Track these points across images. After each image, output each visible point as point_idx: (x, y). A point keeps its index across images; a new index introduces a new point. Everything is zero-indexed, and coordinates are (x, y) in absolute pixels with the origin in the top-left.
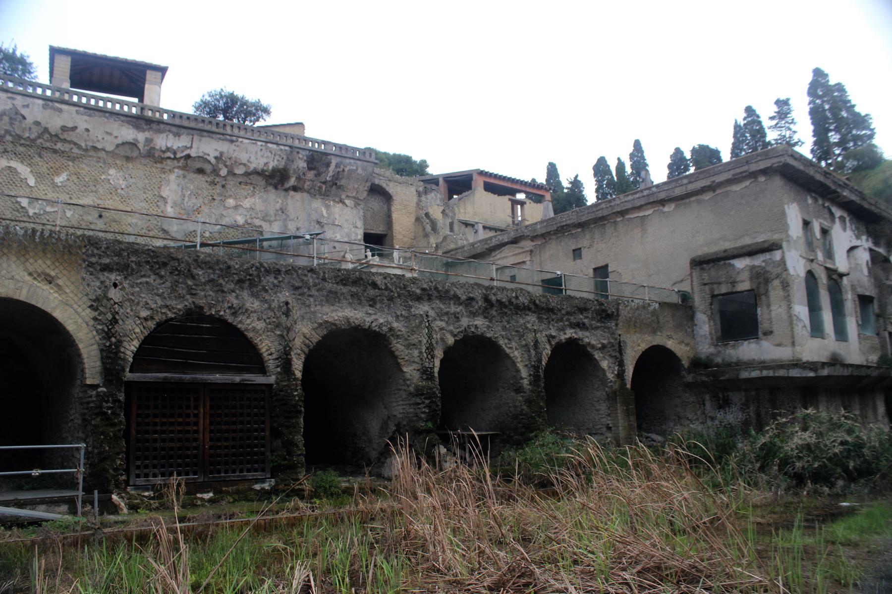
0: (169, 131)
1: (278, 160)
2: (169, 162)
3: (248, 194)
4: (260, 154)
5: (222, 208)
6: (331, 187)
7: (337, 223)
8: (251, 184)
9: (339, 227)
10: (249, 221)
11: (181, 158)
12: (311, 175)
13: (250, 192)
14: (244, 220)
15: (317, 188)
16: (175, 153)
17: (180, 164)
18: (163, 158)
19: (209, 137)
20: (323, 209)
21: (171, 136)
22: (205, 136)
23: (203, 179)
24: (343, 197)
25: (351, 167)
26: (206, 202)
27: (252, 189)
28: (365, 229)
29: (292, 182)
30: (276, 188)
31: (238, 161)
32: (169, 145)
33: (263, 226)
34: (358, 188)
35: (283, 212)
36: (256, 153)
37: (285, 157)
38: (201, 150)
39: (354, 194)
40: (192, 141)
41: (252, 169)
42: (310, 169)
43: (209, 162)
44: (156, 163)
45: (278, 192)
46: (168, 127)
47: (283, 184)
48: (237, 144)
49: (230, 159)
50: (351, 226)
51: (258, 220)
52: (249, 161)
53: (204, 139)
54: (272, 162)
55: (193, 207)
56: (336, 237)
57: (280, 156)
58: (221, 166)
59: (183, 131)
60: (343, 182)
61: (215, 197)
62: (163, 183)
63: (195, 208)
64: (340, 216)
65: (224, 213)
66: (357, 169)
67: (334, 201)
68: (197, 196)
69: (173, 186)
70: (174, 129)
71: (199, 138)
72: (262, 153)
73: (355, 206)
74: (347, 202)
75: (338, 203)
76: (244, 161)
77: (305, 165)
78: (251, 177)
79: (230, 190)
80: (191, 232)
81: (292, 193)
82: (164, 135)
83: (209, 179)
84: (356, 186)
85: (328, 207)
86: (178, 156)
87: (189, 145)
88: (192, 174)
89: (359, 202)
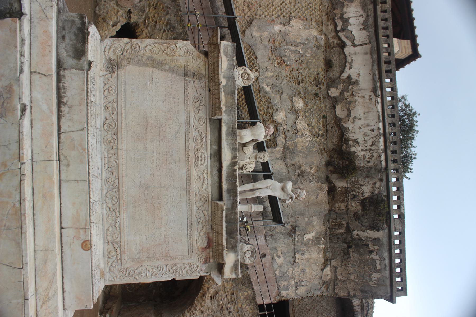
0: (368, 16)
1: (364, 157)
2: (331, 27)
3: (313, 128)
4: (367, 130)
5: (291, 93)
6: (345, 241)
7: (297, 256)
8: (327, 132)
9: (292, 260)
10: (280, 129)
11: (340, 39)
12: (355, 206)
13: (317, 130)
14: (280, 121)
15: (338, 221)
16: (343, 30)
17: (331, 40)
18: (334, 20)
19: (373, 62)
20: (313, 234)
21: (362, 20)
22: (372, 58)
23: (320, 70)
24: (334, 263)
25: (378, 262)
26: (294, 73)
27: (320, 132)
28: (293, 300)
29: (341, 184)
30: (328, 164)
31: (352, 105)
32: (351, 21)
33: (278, 149)
34: (351, 281)
35: (299, 175)
36: (368, 125)
37: (371, 164)
38: (354, 57)
39: (340, 278)
40: (362, 45)
41: (345, 125)
42: (363, 203)
43: (342, 71)
44: (327, 14)
45: (323, 168)
46: (371, 13)
47: (333, 172)
48: (373, 97)
49: (352, 94)
50: (296, 279)
51: (283, 140)
52: (355, 118)
53: (368, 56)
54: (360, 149)
55: (285, 56)
56: (279, 257)
57: (371, 157)
58: (341, 86)
59: (372, 30)
60: (354, 255)
61: (301, 84)
62: (306, 22)
63: (284, 58)
64: (308, 260)
65: (285, 95)
66: (377, 271)
67: (326, 250)
68: (299, 61)
69: (305, 34)
70: (371, 20)
71: (369, 51)
72: (369, 133)
73: (324, 282)
74: (328, 270)
75: (324, 256)
76: (353, 114)
77: (366, 195)
78: (335, 129)
79: (314, 104)
80: (254, 54)
81: (325, 187)
82: (361, 12)
83: (321, 76)
84: (352, 277)
85: (316, 241)
86: (341, 34)
87: (356, 43)
88: (323, 56)
89: (330, 288)
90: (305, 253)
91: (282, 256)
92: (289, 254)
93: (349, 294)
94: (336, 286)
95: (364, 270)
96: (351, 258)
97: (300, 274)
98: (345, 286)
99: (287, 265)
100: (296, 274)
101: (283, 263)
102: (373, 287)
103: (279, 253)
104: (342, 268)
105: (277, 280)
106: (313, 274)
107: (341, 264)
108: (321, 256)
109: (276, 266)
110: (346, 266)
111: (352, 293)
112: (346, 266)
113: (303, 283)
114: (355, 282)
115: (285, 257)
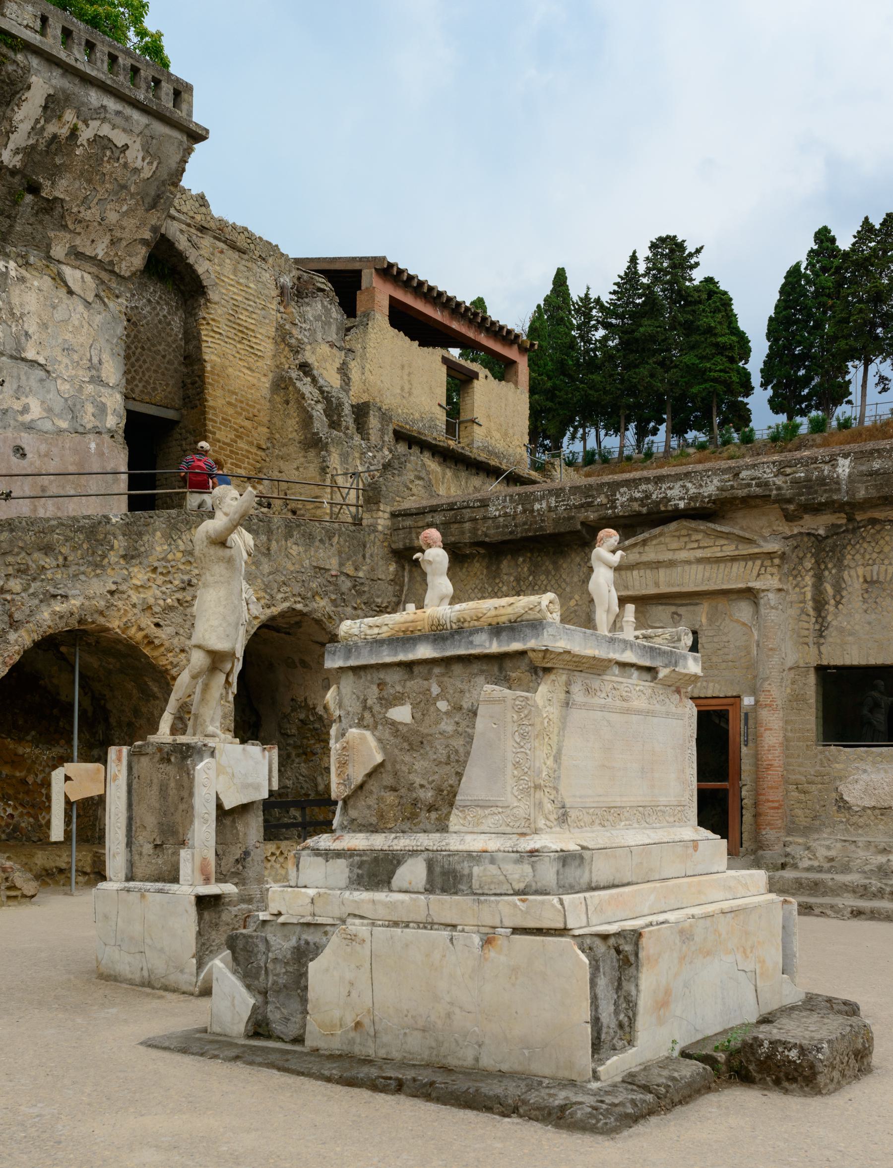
56: (26, 410)
64: (44, 326)
90: (26, 327)
91: (24, 400)
92: (23, 377)
93: (144, 242)
94: (116, 269)
95: (107, 177)
96: (67, 199)
97: (72, 361)
98: (124, 243)
99: (48, 392)
100: (74, 372)
101: (43, 402)
102: (154, 172)
103: (17, 406)
104: (79, 234)
105: (81, 430)
106: (77, 323)
107: (71, 231)
108: (36, 283)
109: (47, 426)
110: (80, 222)
111: (147, 235)
112: (80, 222)
113: (95, 360)
114: (125, 214)
115: (27, 388)
